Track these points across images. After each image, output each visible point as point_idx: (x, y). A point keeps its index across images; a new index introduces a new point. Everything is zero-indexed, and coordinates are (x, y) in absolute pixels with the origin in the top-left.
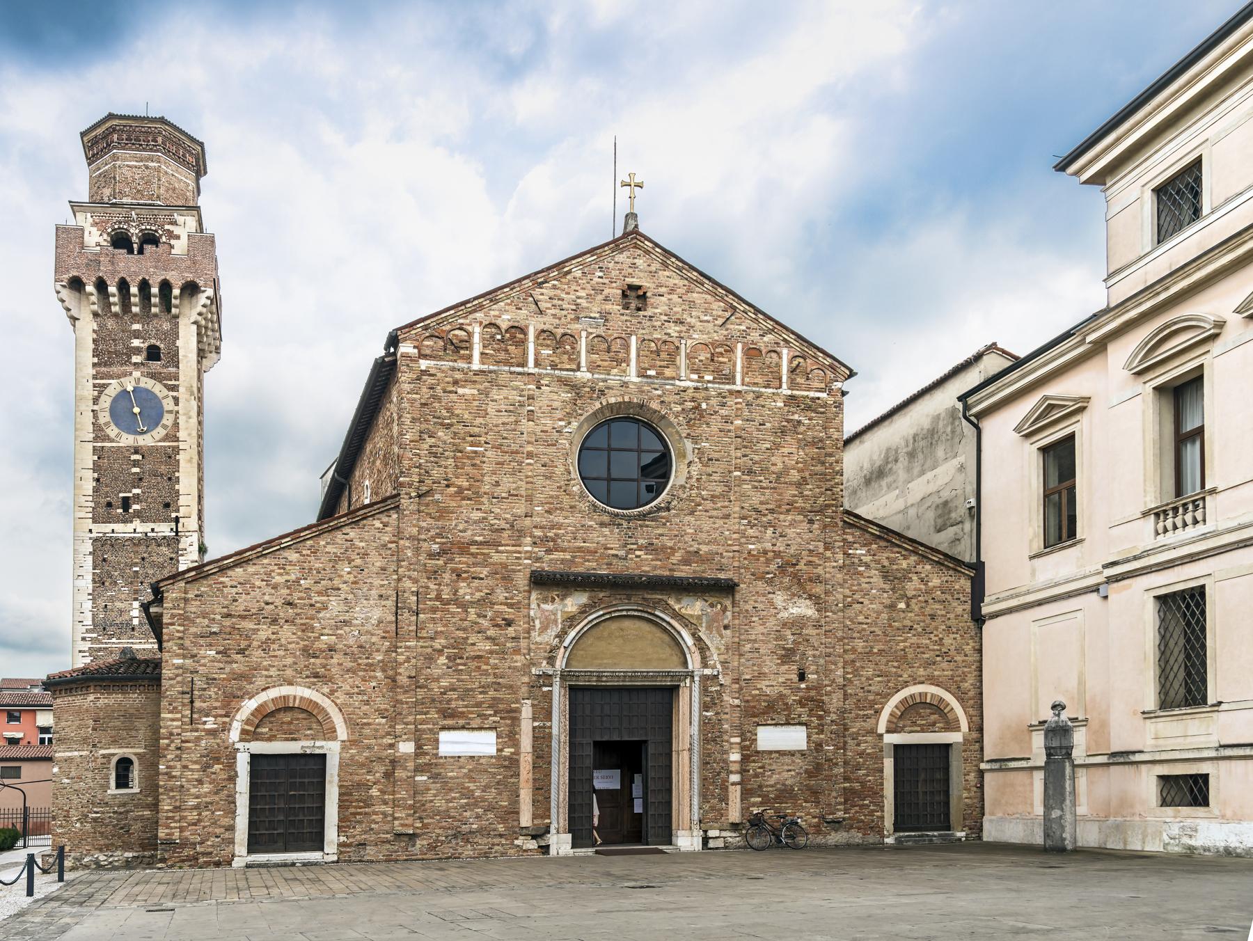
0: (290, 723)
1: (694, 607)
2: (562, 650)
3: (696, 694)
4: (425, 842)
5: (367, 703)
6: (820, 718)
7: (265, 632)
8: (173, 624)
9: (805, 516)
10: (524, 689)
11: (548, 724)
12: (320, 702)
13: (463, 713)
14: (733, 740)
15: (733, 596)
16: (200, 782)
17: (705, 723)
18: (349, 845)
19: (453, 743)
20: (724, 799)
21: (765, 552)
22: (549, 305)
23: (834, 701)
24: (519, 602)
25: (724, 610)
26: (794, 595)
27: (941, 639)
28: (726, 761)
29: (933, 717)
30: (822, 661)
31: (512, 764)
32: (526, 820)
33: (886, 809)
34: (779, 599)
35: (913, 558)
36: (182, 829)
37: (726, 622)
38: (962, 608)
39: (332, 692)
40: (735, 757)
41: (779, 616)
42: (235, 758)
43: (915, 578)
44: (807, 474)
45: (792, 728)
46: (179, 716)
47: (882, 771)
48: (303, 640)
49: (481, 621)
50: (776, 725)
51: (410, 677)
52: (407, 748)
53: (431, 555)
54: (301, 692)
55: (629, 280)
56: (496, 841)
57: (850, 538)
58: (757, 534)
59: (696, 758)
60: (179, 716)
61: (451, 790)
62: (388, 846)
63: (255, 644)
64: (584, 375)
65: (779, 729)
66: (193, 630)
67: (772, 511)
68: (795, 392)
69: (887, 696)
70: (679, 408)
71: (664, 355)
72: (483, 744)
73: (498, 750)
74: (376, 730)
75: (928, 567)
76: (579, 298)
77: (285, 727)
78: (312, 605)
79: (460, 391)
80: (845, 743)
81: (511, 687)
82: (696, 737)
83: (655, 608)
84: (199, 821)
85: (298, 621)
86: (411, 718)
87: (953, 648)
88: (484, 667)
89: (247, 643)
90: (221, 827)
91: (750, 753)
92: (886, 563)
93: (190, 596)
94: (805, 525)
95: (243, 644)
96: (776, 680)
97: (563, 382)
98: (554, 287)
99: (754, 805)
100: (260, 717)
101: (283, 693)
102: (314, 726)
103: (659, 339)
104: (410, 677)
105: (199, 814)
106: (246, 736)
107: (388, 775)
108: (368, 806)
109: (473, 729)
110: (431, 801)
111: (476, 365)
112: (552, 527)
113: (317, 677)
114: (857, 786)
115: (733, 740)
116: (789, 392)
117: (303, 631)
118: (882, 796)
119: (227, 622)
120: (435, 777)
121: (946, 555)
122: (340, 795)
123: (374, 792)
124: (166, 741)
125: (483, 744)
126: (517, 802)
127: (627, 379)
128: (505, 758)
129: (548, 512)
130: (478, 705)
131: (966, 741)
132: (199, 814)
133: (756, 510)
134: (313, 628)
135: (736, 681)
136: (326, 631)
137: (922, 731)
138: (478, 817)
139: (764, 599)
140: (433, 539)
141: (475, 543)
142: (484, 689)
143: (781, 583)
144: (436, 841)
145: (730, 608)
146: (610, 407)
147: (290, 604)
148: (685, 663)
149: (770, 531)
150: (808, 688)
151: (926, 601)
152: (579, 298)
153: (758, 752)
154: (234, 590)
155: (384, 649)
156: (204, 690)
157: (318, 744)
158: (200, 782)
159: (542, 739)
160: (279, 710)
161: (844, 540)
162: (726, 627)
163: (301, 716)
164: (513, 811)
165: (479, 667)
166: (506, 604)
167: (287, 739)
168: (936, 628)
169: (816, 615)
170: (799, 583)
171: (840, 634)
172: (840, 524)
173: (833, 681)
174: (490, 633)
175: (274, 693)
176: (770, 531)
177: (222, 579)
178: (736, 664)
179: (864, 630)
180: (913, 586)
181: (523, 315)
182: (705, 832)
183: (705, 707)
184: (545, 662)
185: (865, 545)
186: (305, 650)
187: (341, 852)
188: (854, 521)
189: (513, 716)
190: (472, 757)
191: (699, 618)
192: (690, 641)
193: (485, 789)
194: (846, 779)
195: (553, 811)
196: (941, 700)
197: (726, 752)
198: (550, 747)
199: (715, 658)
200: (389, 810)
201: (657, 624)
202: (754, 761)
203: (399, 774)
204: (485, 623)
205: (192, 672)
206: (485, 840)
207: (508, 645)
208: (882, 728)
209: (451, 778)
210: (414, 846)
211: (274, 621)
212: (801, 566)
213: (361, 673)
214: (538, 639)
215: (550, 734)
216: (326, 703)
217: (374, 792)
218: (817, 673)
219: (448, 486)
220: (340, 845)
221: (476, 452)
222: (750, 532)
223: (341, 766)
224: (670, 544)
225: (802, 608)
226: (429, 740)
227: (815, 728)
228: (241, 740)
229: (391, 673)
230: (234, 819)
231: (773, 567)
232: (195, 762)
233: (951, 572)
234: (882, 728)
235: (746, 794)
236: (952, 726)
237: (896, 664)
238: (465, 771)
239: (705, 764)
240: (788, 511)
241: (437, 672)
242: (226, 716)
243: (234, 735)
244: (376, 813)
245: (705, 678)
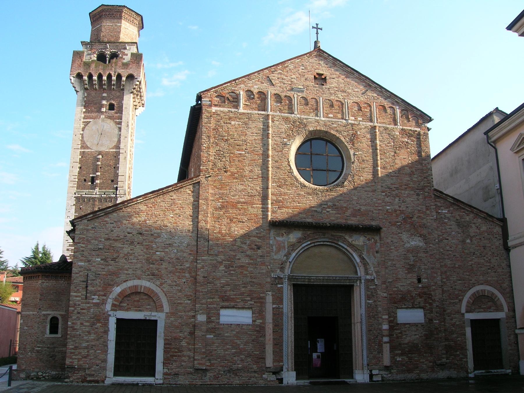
0: (138, 301)
1: (359, 240)
2: (288, 263)
3: (363, 290)
4: (212, 374)
5: (180, 291)
6: (431, 304)
7: (127, 249)
8: (79, 243)
9: (415, 192)
10: (268, 285)
11: (281, 306)
12: (154, 289)
13: (233, 298)
14: (384, 317)
15: (380, 234)
16: (89, 333)
17: (369, 307)
18: (169, 374)
19: (229, 316)
20: (380, 351)
21: (396, 211)
22: (278, 82)
23: (437, 295)
24: (264, 236)
25: (376, 242)
26: (412, 235)
27: (490, 260)
28: (381, 330)
29: (490, 304)
30: (429, 272)
31: (260, 330)
32: (269, 362)
33: (468, 357)
34: (405, 236)
35: (472, 215)
36: (79, 360)
37: (377, 249)
38: (499, 243)
39: (161, 284)
40: (385, 327)
41: (405, 246)
42: (108, 320)
43: (473, 226)
44: (414, 169)
45: (416, 310)
46: (80, 294)
47: (465, 335)
48: (146, 254)
49: (243, 246)
50: (407, 308)
51: (204, 277)
52: (202, 318)
53: (216, 209)
54: (145, 284)
55: (317, 71)
56: (253, 375)
57: (439, 204)
58: (390, 201)
59: (364, 327)
60: (80, 294)
61: (226, 344)
62: (191, 376)
63: (121, 255)
64: (296, 115)
65: (409, 310)
66: (89, 246)
67: (397, 189)
68: (404, 127)
69: (465, 292)
70: (346, 134)
71: (336, 107)
72: (243, 317)
73: (253, 321)
74: (185, 307)
75: (480, 220)
76: (292, 78)
77: (136, 303)
78: (152, 235)
79: (233, 123)
80: (445, 319)
81: (260, 284)
82: (364, 315)
83: (338, 241)
84: (88, 355)
85: (145, 243)
86: (204, 301)
87: (496, 264)
88: (245, 272)
89: (117, 255)
90: (99, 360)
91: (394, 325)
92: (458, 218)
93: (89, 228)
94: (415, 197)
95: (115, 255)
96: (406, 283)
97: (286, 120)
98: (281, 74)
99: (397, 355)
100: (122, 297)
101: (135, 284)
102: (152, 303)
103: (333, 99)
104: (204, 277)
106: (115, 307)
107: (192, 333)
108: (180, 351)
109: (239, 308)
110: (215, 350)
111: (241, 110)
112: (281, 195)
113: (154, 276)
114: (452, 343)
115: (384, 317)
116: (401, 127)
117: (147, 249)
118: (466, 350)
119: (108, 243)
120: (217, 336)
121: (487, 214)
122: (165, 344)
123: (184, 343)
124: (72, 309)
125: (243, 317)
126: (264, 352)
127: (318, 118)
128: (257, 326)
129: (279, 186)
130: (242, 294)
131: (508, 317)
132: (88, 352)
133: (389, 188)
134: (152, 247)
135: (384, 283)
136: (159, 249)
137: (485, 311)
138: (242, 360)
139: (396, 236)
140: (218, 199)
141: (239, 202)
142: (245, 285)
143: (405, 228)
144: (218, 374)
145: (378, 241)
146: (310, 132)
147: (141, 234)
148: (356, 272)
149: (397, 199)
150: (423, 287)
151: (480, 239)
152: (292, 78)
153: (398, 324)
155: (190, 260)
156: (93, 280)
157: (154, 314)
158: (89, 333)
159: (278, 314)
160: (132, 293)
161: (435, 205)
162: (377, 252)
163: (144, 297)
164: (262, 358)
165: (242, 272)
166: (257, 237)
167: (136, 311)
168: (487, 254)
169: (425, 246)
170: (414, 228)
171: (437, 256)
172: (433, 196)
173: (436, 283)
174: (249, 253)
175: (130, 284)
176: (397, 199)
177: (106, 219)
178: (383, 273)
179: (450, 254)
180: (473, 230)
181: (265, 87)
182: (371, 371)
183: (368, 297)
184: (279, 270)
185: (447, 208)
186: (147, 260)
187: (165, 378)
188: (439, 195)
189: (261, 301)
190: (237, 324)
191: (362, 246)
192: (358, 260)
193: (246, 343)
194: (447, 339)
195: (285, 358)
196: (493, 294)
197: (381, 324)
198: (282, 319)
199: (372, 269)
200: (192, 354)
201: (340, 250)
202: (396, 329)
203: (198, 333)
204: (245, 247)
205: (87, 270)
206: (246, 374)
207: (258, 260)
208: (463, 310)
209: (227, 337)
210: (205, 376)
211: (132, 243)
212: (415, 219)
213: (177, 274)
214: (275, 257)
215: (282, 313)
216: (157, 290)
217: (184, 343)
218: (427, 278)
219: (226, 172)
220: (165, 374)
221: (240, 154)
222: (387, 199)
223: (166, 328)
224: (345, 205)
225: (416, 242)
226: (214, 314)
227: (428, 311)
228: (112, 310)
229: (193, 274)
230: (106, 355)
231: (400, 219)
232: (87, 321)
233: (491, 223)
234: (463, 310)
235: (392, 349)
236: (499, 308)
237: (468, 273)
238: (234, 333)
239: (369, 331)
240: (406, 188)
241: (219, 274)
242: (104, 296)
243: (108, 307)
244: (185, 356)
245: (367, 281)
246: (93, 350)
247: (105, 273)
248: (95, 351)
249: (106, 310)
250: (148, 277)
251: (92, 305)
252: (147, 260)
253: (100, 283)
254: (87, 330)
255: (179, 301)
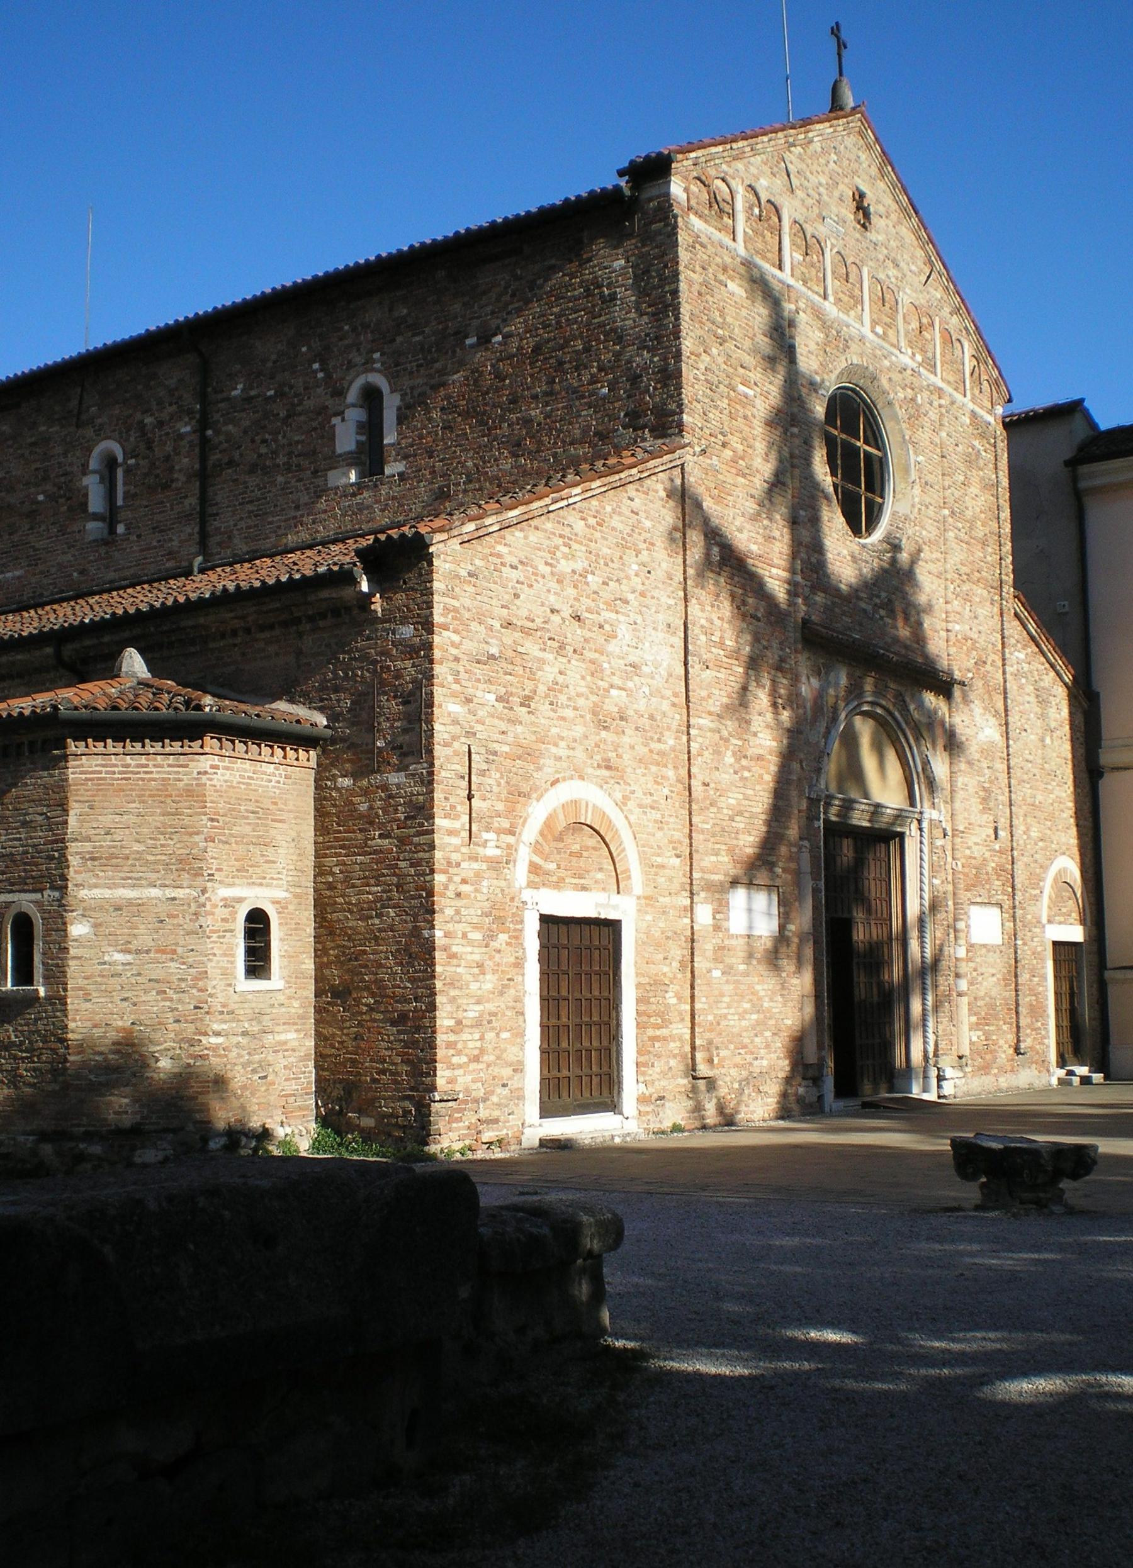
105: (482, 1039)
154: (515, 575)
213: (654, 768)
223: (640, 945)
242: (511, 832)
243: (520, 873)
246: (493, 1029)
247: (506, 749)
248: (498, 1035)
249: (517, 885)
250: (599, 772)
251: (484, 866)
252: (595, 713)
253: (499, 785)
254: (477, 957)
255: (659, 860)
